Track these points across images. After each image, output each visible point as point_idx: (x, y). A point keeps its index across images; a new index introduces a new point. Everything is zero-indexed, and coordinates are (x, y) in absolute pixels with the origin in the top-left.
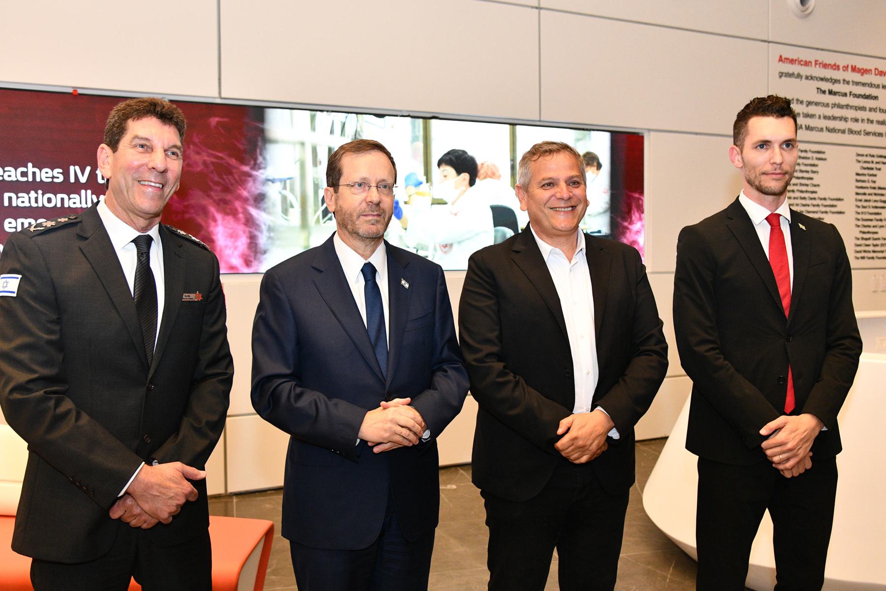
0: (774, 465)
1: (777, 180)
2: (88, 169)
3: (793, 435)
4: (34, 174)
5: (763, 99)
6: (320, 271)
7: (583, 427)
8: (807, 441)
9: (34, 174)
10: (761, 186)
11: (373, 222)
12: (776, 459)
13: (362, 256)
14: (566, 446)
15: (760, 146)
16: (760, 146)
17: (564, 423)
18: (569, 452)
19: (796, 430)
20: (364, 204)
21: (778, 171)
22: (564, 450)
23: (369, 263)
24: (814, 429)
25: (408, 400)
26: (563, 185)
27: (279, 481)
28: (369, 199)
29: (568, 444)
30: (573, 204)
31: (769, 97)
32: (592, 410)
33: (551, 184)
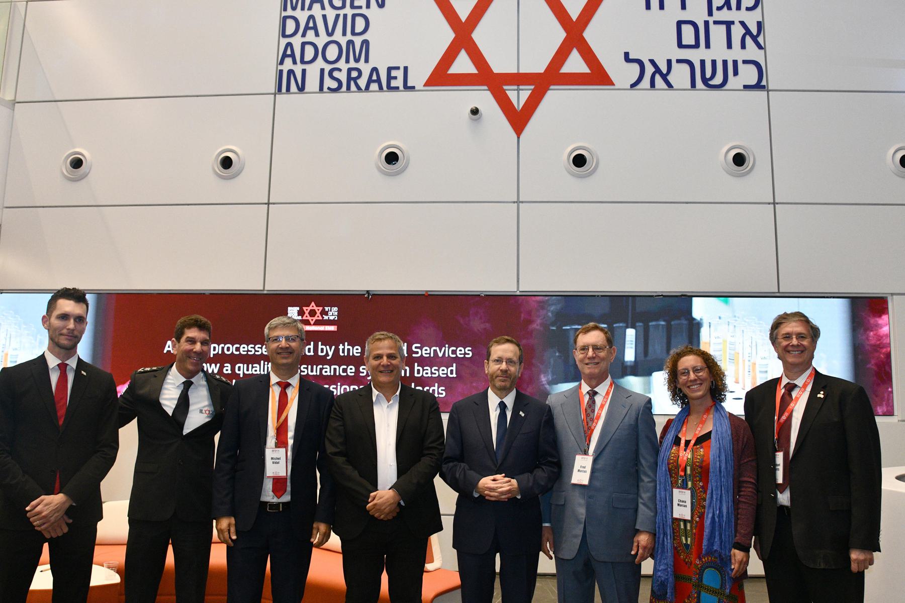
0: (36, 528)
1: (69, 340)
2: (333, 347)
3: (47, 507)
4: (349, 350)
5: (70, 289)
6: (477, 405)
7: (381, 498)
8: (58, 512)
9: (349, 350)
10: (58, 342)
11: (503, 380)
12: (35, 524)
13: (500, 398)
14: (371, 508)
15: (62, 317)
16: (62, 317)
17: (372, 494)
18: (373, 512)
19: (51, 504)
20: (499, 371)
21: (71, 335)
22: (371, 510)
23: (503, 401)
24: (64, 503)
25: (504, 475)
26: (385, 358)
27: (454, 513)
28: (501, 368)
29: (372, 507)
30: (391, 369)
31: (73, 288)
32: (390, 489)
33: (379, 357)
